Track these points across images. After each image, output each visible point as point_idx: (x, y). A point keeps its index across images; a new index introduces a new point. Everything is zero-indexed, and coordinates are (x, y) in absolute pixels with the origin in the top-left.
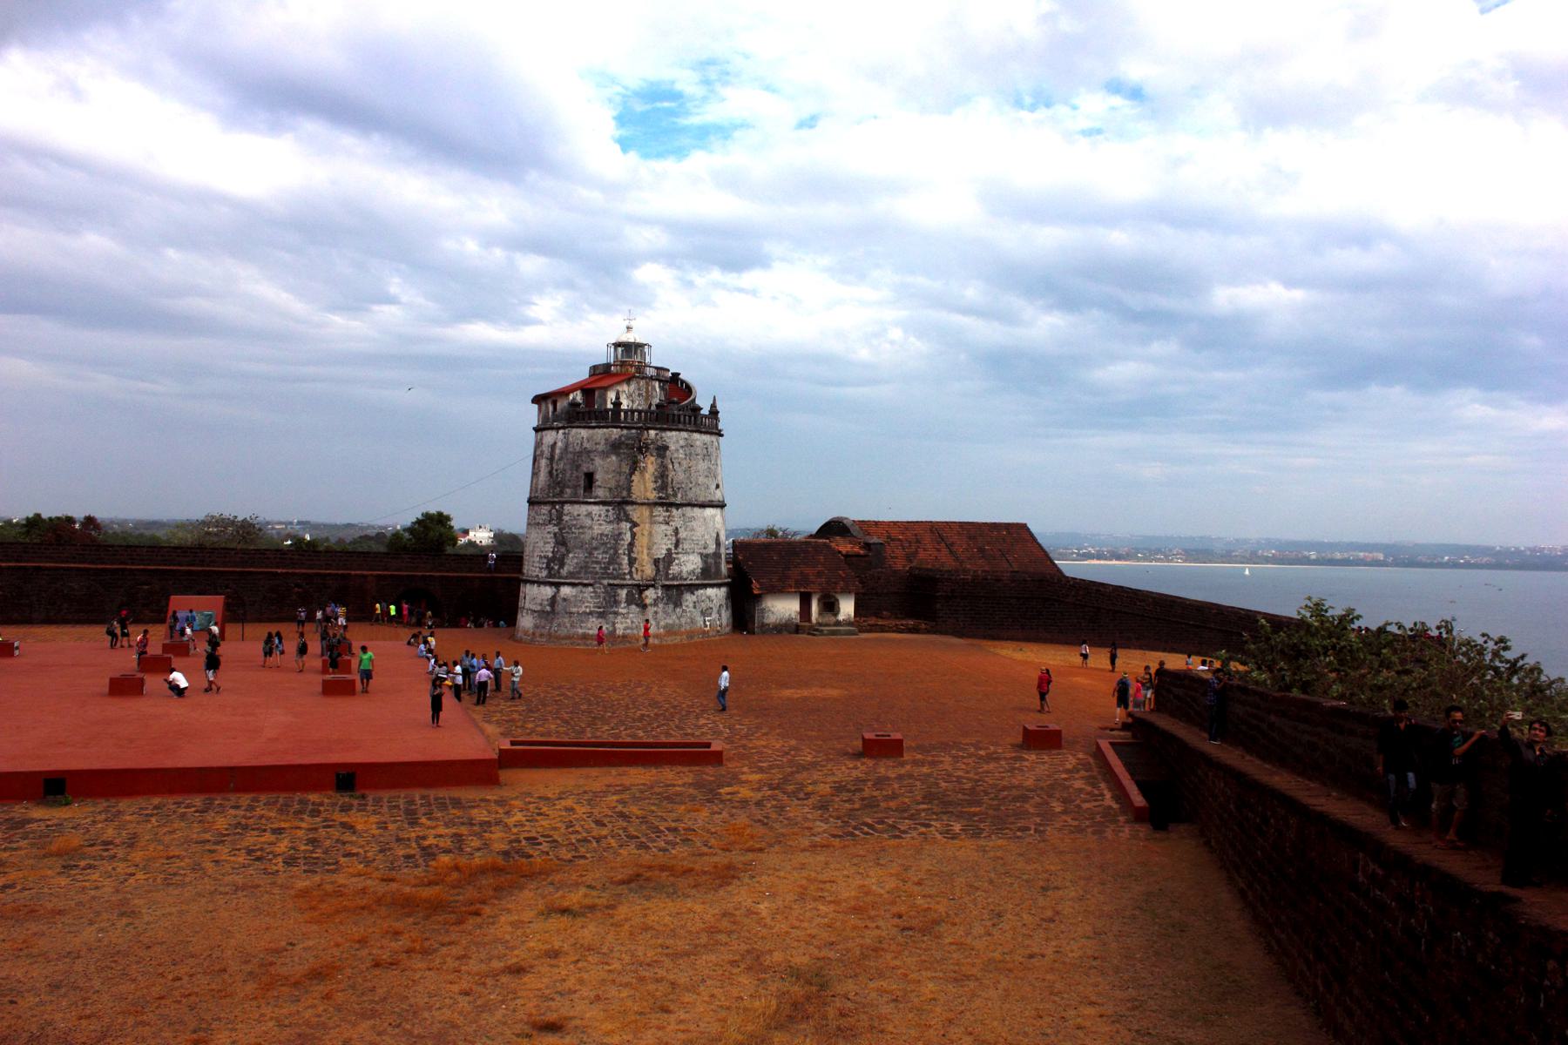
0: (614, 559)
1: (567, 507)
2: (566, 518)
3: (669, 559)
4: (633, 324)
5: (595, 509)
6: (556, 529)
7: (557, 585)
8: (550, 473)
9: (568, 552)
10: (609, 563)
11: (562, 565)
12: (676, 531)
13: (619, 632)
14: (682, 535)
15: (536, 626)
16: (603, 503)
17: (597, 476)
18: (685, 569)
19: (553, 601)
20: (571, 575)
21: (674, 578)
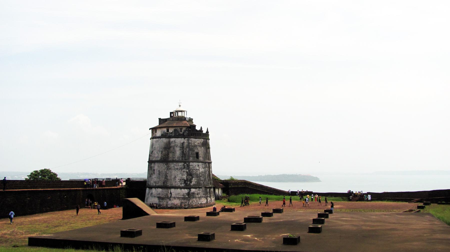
1: (191, 164)
4: (181, 104)
5: (200, 164)
6: (188, 171)
7: (190, 189)
8: (183, 152)
9: (192, 178)
10: (205, 181)
11: (191, 182)
15: (182, 203)
16: (202, 162)
17: (199, 154)
19: (188, 194)
20: (194, 185)
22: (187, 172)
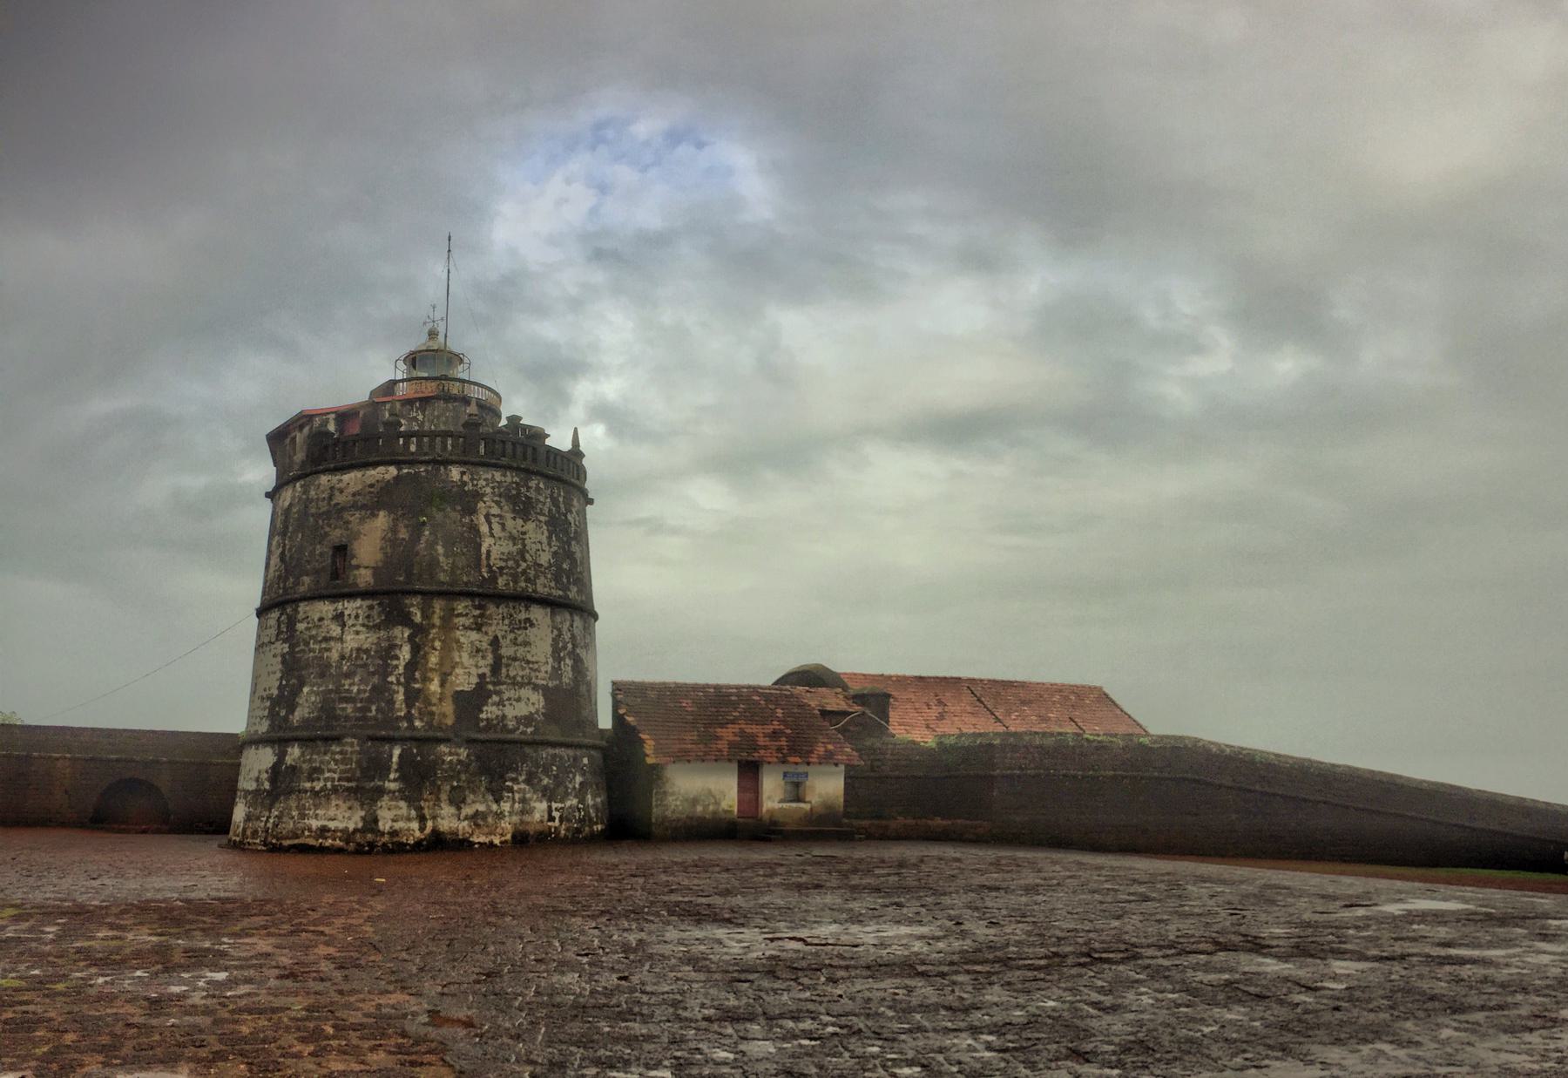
0: (381, 692)
1: (302, 607)
2: (301, 626)
3: (480, 694)
5: (350, 607)
9: (302, 684)
10: (370, 701)
11: (291, 710)
12: (495, 643)
13: (385, 825)
14: (507, 650)
16: (364, 595)
18: (512, 712)
20: (306, 723)
21: (490, 725)
22: (283, 656)
